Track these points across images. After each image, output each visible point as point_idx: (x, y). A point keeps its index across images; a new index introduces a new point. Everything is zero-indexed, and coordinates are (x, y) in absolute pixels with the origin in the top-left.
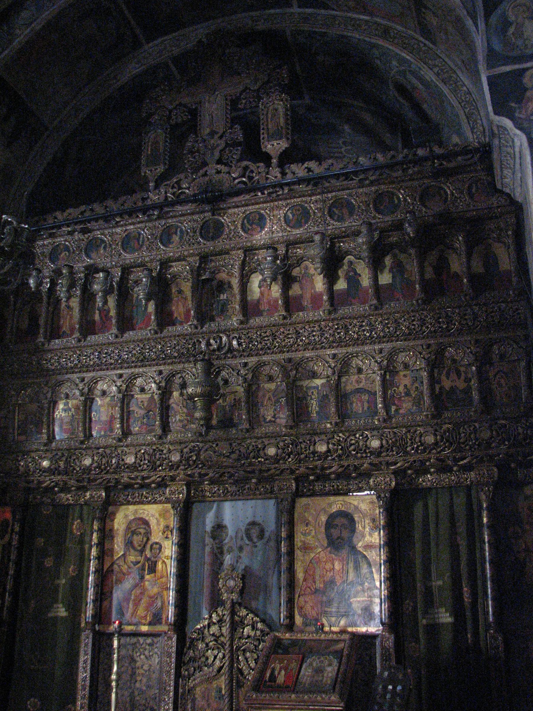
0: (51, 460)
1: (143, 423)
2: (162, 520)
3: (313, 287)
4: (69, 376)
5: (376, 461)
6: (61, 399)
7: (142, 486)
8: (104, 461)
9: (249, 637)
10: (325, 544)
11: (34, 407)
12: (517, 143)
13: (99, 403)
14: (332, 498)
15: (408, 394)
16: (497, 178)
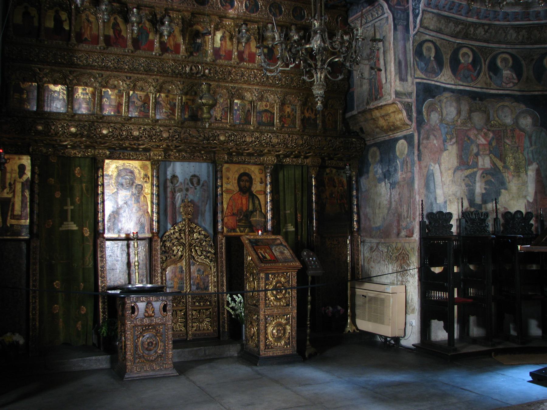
0: (76, 127)
1: (141, 111)
2: (142, 171)
3: (250, 48)
4: (90, 71)
5: (271, 149)
6: (81, 86)
7: (133, 149)
8: (117, 132)
9: (197, 238)
10: (238, 189)
11: (58, 88)
12: (386, 15)
13: (110, 93)
14: (241, 166)
15: (289, 116)
16: (350, 19)
